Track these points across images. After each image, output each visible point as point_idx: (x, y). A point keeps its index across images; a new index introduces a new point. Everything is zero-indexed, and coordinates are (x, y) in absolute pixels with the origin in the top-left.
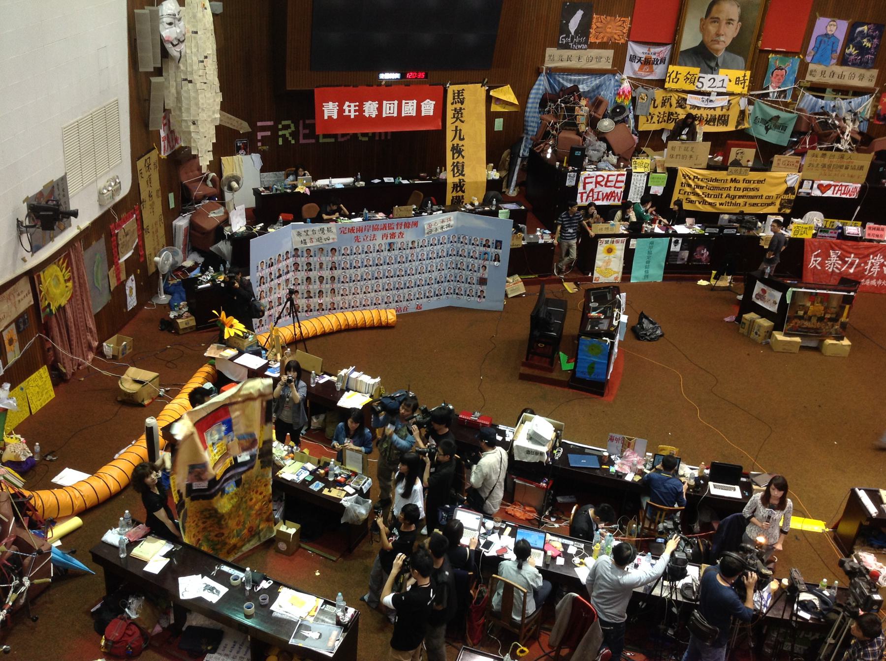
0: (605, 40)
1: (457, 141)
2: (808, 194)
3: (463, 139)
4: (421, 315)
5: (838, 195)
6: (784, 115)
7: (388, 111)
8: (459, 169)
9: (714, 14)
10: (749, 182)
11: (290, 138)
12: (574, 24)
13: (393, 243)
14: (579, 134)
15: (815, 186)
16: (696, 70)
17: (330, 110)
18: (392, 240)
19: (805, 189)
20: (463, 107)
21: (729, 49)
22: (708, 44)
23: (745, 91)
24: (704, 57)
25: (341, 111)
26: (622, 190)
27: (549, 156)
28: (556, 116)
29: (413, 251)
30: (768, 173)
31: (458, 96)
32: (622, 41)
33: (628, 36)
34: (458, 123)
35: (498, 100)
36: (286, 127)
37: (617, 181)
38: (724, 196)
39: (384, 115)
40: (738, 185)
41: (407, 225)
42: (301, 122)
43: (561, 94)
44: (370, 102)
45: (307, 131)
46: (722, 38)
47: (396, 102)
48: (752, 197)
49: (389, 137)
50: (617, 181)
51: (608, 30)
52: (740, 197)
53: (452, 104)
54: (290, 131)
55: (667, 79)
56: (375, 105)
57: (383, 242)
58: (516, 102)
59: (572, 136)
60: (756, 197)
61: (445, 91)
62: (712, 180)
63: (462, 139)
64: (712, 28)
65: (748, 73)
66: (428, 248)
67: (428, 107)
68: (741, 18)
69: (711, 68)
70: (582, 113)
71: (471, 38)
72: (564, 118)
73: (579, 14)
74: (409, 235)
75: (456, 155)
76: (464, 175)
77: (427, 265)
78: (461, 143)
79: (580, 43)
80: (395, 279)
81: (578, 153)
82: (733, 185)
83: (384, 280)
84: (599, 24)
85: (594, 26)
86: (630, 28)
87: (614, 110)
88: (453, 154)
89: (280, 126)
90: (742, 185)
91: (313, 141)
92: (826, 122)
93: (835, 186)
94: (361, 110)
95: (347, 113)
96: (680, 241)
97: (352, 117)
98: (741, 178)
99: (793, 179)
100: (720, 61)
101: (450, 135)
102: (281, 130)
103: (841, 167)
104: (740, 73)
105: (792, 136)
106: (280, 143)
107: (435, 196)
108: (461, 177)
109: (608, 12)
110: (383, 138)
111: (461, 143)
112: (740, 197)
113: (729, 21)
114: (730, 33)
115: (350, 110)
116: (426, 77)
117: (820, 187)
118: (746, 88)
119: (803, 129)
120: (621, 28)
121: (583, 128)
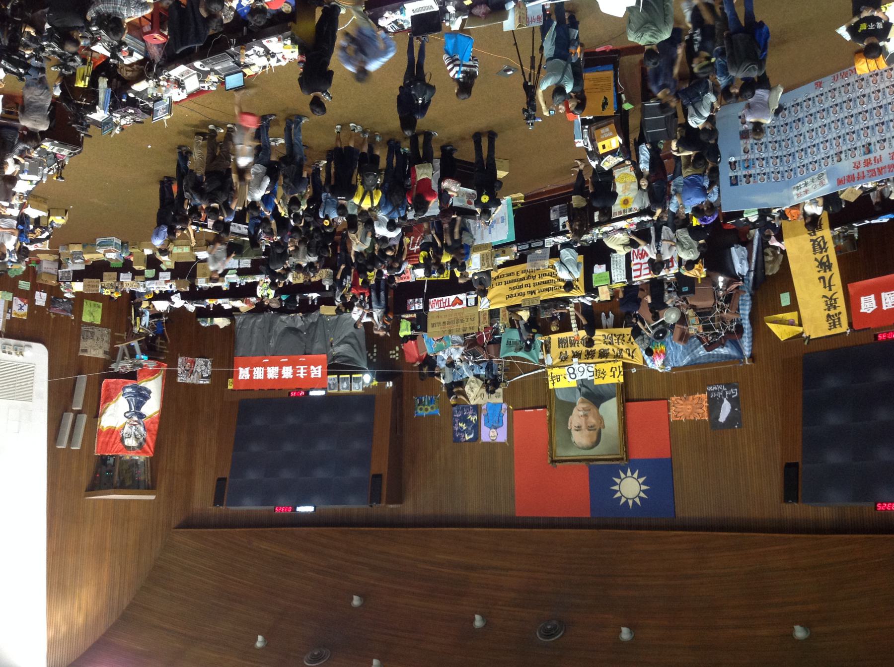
0: (691, 397)
1: (827, 275)
2: (468, 294)
3: (820, 279)
4: (816, 78)
5: (444, 298)
6: (513, 354)
8: (819, 246)
9: (594, 434)
10: (519, 294)
12: (726, 409)
13: (865, 154)
14: (693, 307)
15: (465, 302)
16: (598, 382)
18: (867, 157)
19: (472, 297)
20: (827, 312)
21: (573, 405)
22: (592, 407)
23: (549, 371)
24: (594, 395)
26: (633, 263)
27: (721, 279)
28: (722, 319)
29: (838, 150)
30: (505, 305)
31: (834, 322)
32: (673, 399)
33: (668, 404)
34: (829, 294)
35: (792, 324)
37: (640, 270)
38: (537, 277)
40: (528, 289)
41: (851, 179)
43: (723, 341)
46: (581, 413)
48: (514, 281)
50: (640, 270)
51: (690, 407)
52: (523, 279)
53: (840, 313)
55: (621, 369)
57: (877, 154)
58: (770, 326)
59: (699, 304)
60: (510, 282)
61: (850, 325)
62: (552, 289)
63: (823, 278)
64: (592, 421)
65: (551, 387)
66: (819, 157)
67: (867, 304)
68: (569, 432)
69: (584, 386)
70: (696, 327)
71: (832, 382)
72: (713, 320)
73: (723, 418)
74: (846, 167)
75: (825, 260)
76: (811, 240)
77: (818, 137)
78: (822, 274)
79: (716, 391)
80: (855, 111)
81: (685, 289)
82: (532, 289)
83: (870, 107)
84: (700, 411)
85: (705, 409)
86: (669, 410)
87: (665, 333)
88: (828, 260)
90: (525, 290)
92: (474, 357)
93: (449, 306)
96: (561, 227)
98: (527, 296)
99: (485, 305)
100: (578, 393)
101: (837, 280)
103: (449, 323)
104: (558, 385)
105: (500, 338)
107: (839, 211)
108: (814, 238)
109: (695, 425)
111: (822, 274)
112: (523, 279)
113: (579, 428)
114: (576, 418)
116: (876, 336)
117: (461, 302)
118: (549, 373)
119: (492, 346)
120: (678, 410)
121: (690, 313)
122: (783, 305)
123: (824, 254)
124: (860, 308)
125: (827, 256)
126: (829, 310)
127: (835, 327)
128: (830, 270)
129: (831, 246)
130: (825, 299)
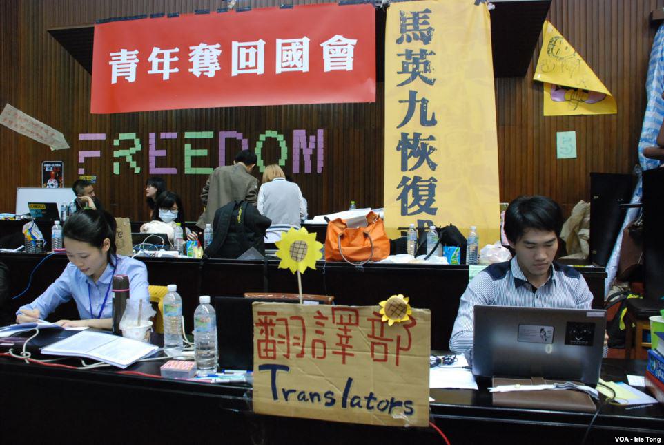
1: (413, 127)
7: (243, 64)
8: (420, 194)
11: (133, 164)
17: (124, 65)
20: (428, 48)
25: (143, 66)
34: (417, 85)
36: (127, 144)
39: (235, 72)
42: (152, 136)
44: (203, 46)
45: (162, 153)
47: (261, 43)
49: (319, 171)
53: (399, 41)
54: (133, 151)
56: (214, 51)
61: (381, 15)
67: (340, 53)
75: (412, 161)
76: (433, 212)
78: (426, 132)
89: (116, 142)
91: (173, 171)
94: (183, 62)
95: (155, 70)
97: (166, 77)
102: (118, 148)
106: (116, 171)
108: (424, 216)
110: (308, 170)
111: (426, 132)
115: (162, 62)
122: (572, 135)
123: (407, 174)
124: (356, 48)
125: (404, 168)
126: (423, 52)
127: (415, 16)
128: (404, 135)
129: (391, 189)
130: (427, 75)
